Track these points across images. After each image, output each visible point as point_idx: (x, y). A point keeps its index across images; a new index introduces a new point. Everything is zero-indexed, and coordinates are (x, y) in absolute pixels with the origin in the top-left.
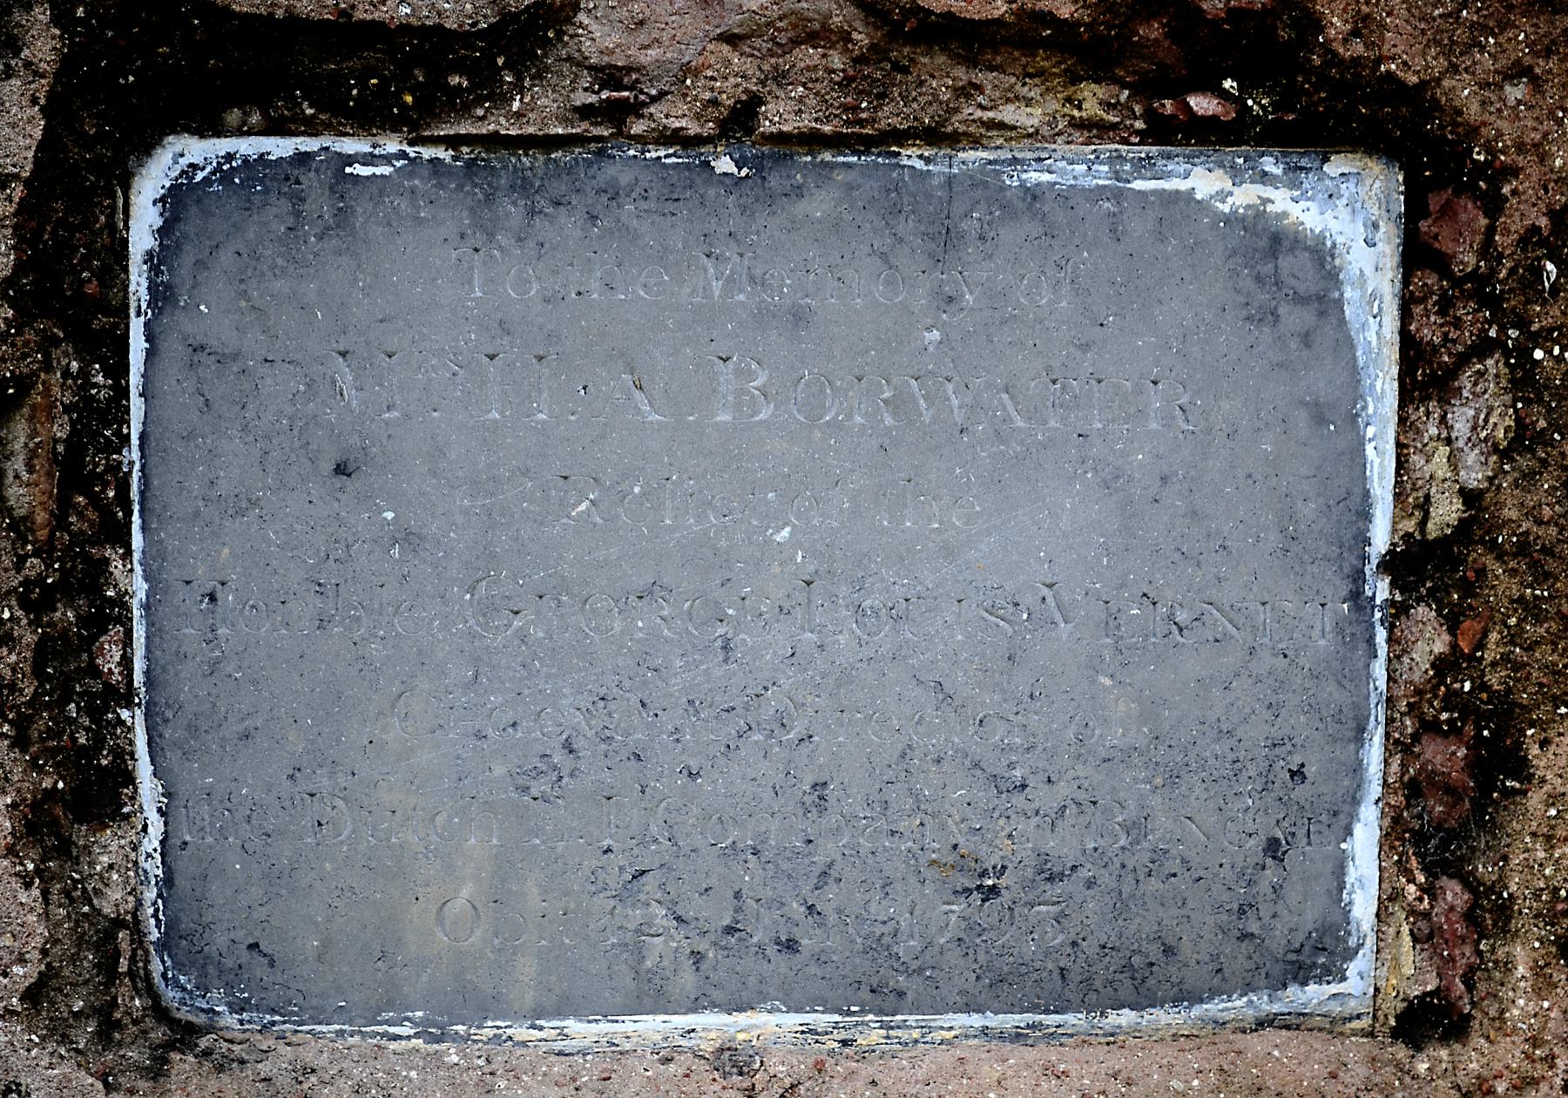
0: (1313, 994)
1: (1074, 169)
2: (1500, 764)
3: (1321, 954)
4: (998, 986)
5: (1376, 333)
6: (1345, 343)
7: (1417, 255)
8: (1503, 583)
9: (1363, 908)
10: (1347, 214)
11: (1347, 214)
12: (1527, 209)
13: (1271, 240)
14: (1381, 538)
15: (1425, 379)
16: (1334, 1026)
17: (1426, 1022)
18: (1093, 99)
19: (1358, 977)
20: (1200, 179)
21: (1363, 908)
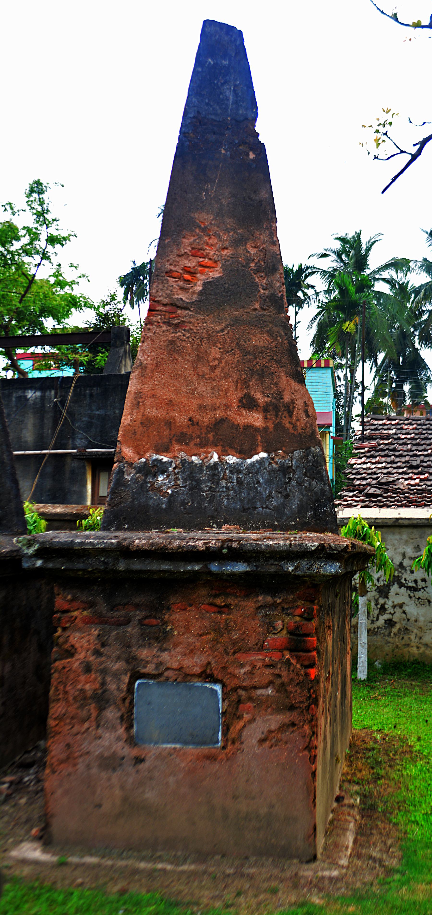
0: (216, 746)
1: (198, 684)
2: (228, 729)
3: (217, 742)
4: (194, 743)
5: (220, 696)
6: (218, 697)
7: (223, 691)
8: (228, 716)
9: (220, 739)
10: (218, 688)
11: (218, 688)
12: (229, 688)
13: (212, 690)
14: (220, 711)
15: (223, 700)
16: (218, 748)
17: (224, 747)
18: (200, 679)
19: (219, 744)
20: (208, 685)
21: (220, 739)
